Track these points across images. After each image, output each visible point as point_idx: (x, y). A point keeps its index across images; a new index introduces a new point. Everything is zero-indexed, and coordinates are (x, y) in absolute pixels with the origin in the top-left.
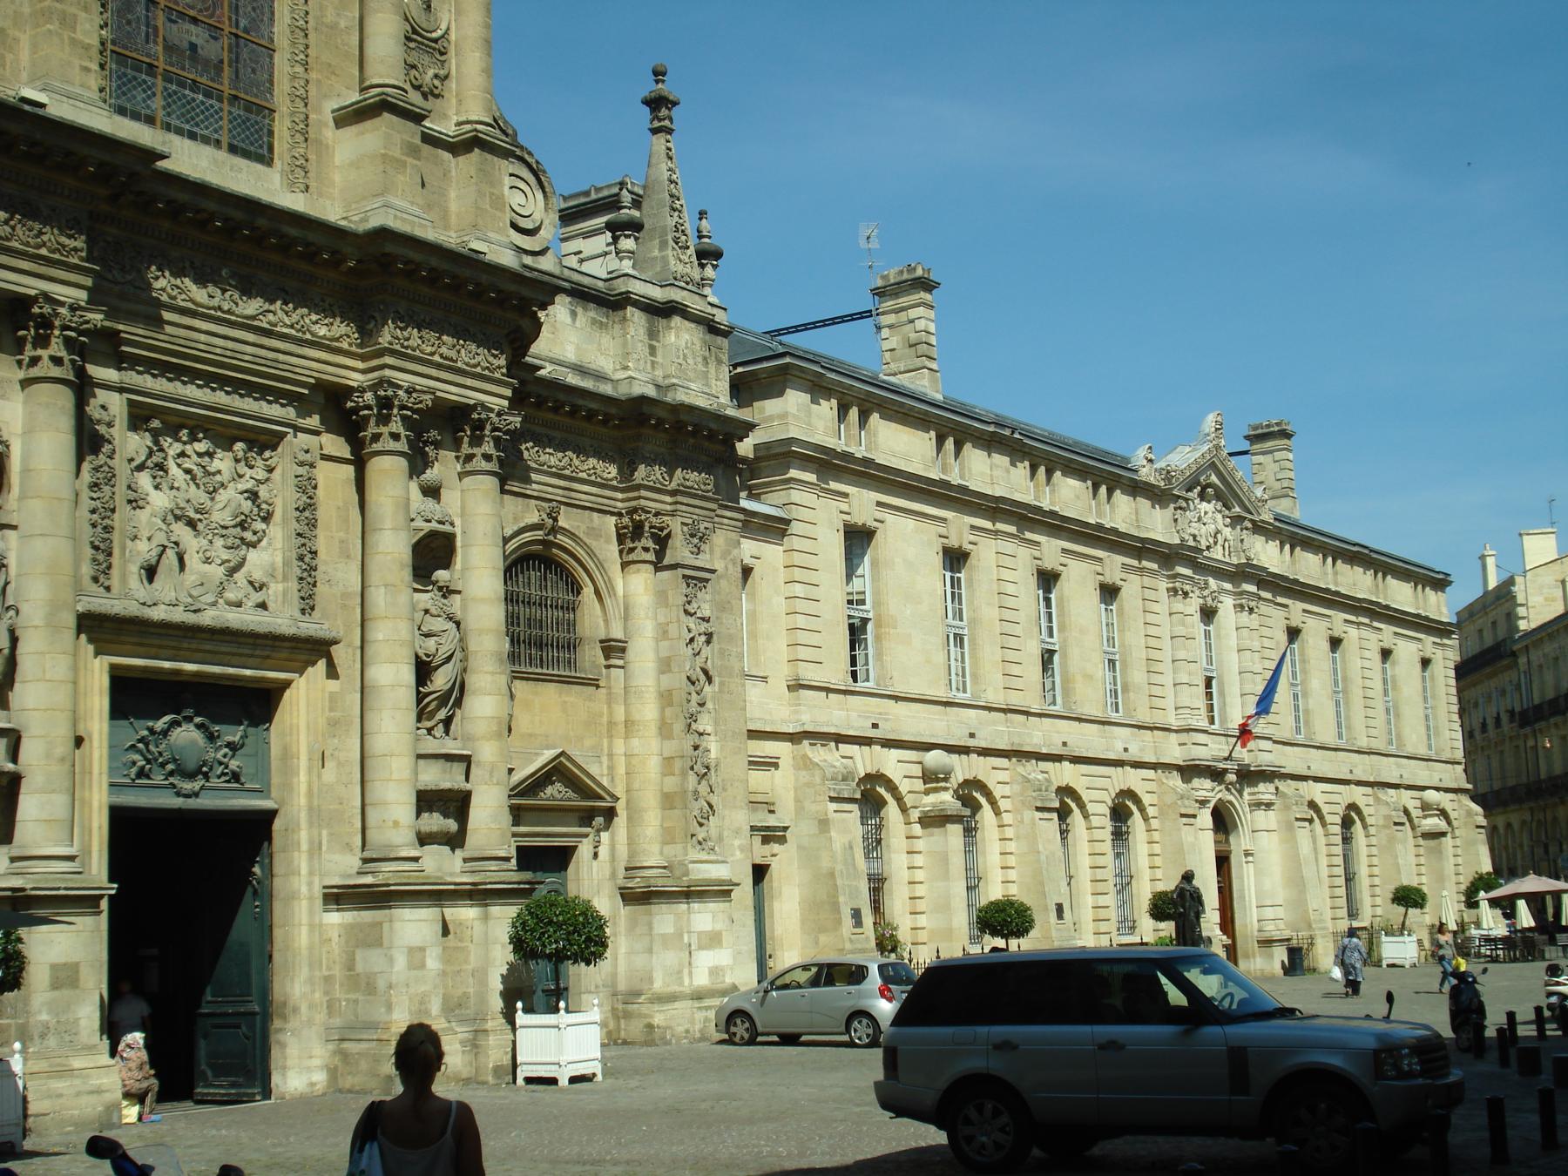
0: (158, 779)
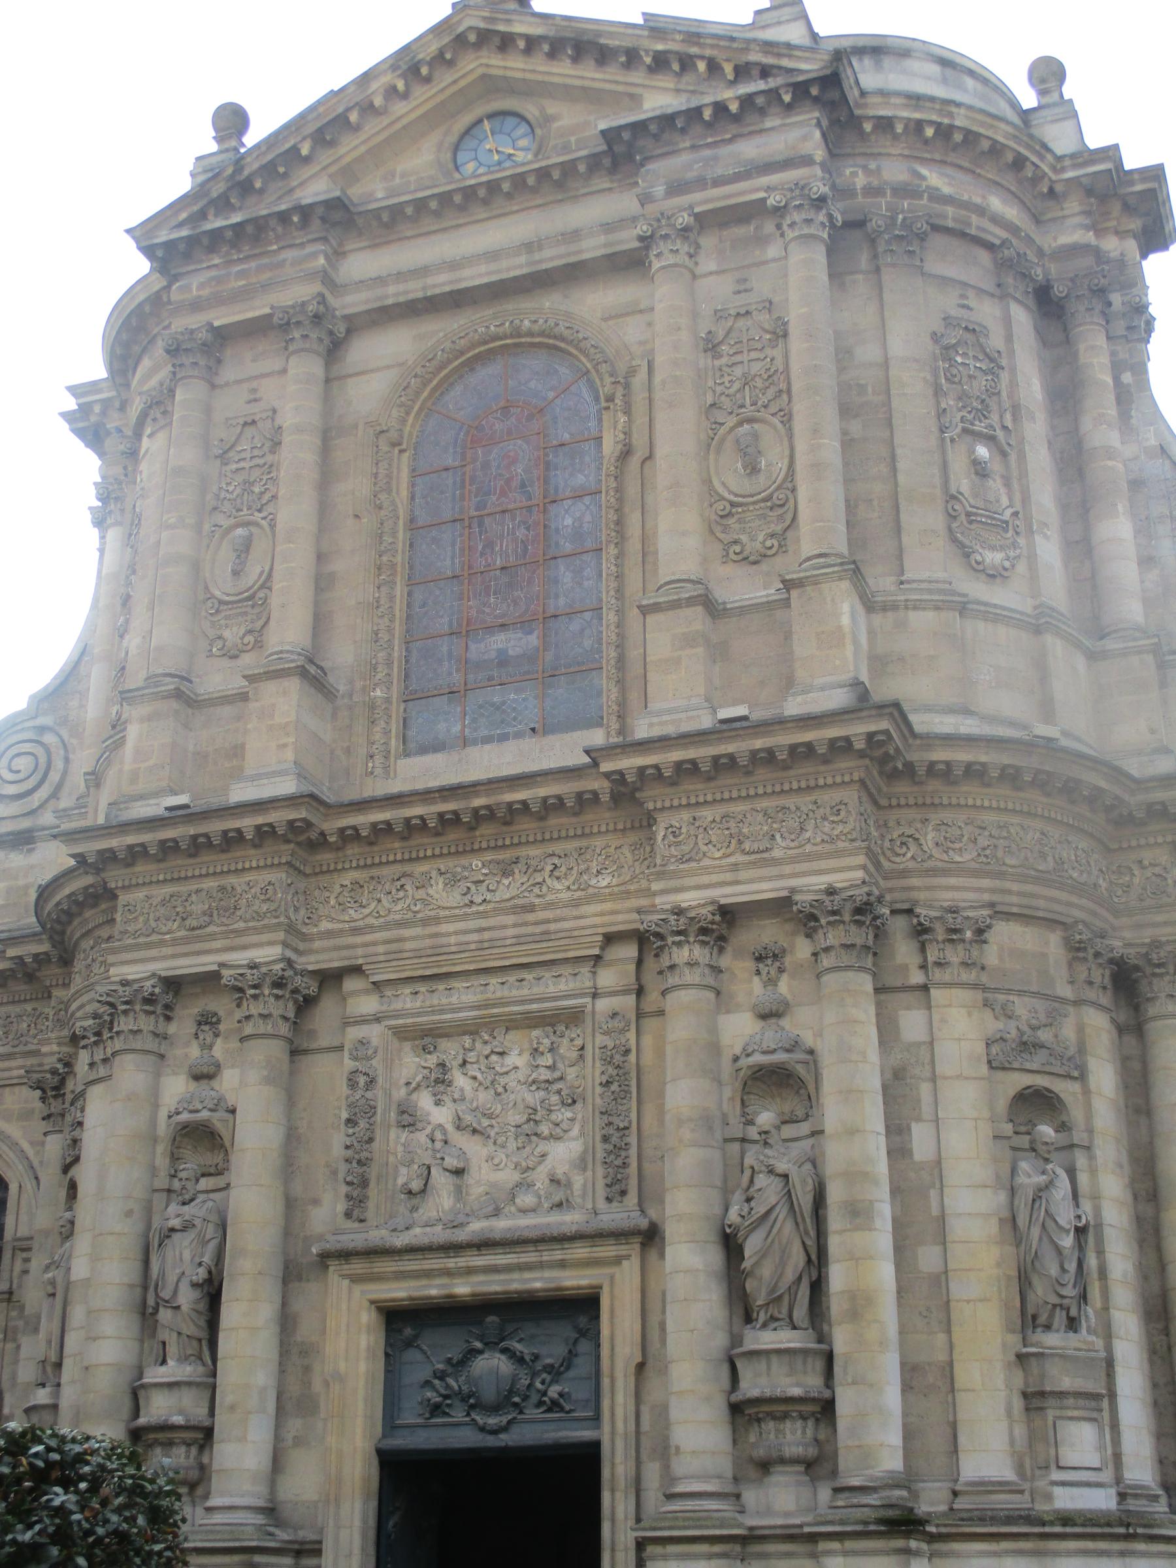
0: (458, 1415)
